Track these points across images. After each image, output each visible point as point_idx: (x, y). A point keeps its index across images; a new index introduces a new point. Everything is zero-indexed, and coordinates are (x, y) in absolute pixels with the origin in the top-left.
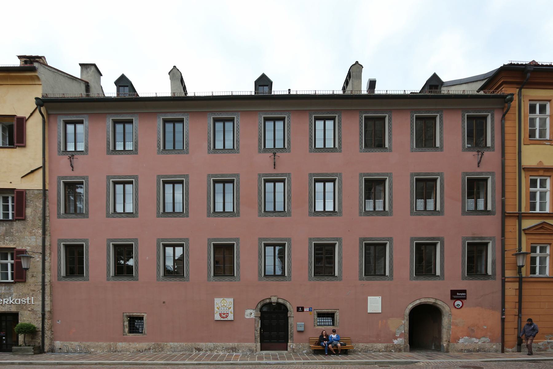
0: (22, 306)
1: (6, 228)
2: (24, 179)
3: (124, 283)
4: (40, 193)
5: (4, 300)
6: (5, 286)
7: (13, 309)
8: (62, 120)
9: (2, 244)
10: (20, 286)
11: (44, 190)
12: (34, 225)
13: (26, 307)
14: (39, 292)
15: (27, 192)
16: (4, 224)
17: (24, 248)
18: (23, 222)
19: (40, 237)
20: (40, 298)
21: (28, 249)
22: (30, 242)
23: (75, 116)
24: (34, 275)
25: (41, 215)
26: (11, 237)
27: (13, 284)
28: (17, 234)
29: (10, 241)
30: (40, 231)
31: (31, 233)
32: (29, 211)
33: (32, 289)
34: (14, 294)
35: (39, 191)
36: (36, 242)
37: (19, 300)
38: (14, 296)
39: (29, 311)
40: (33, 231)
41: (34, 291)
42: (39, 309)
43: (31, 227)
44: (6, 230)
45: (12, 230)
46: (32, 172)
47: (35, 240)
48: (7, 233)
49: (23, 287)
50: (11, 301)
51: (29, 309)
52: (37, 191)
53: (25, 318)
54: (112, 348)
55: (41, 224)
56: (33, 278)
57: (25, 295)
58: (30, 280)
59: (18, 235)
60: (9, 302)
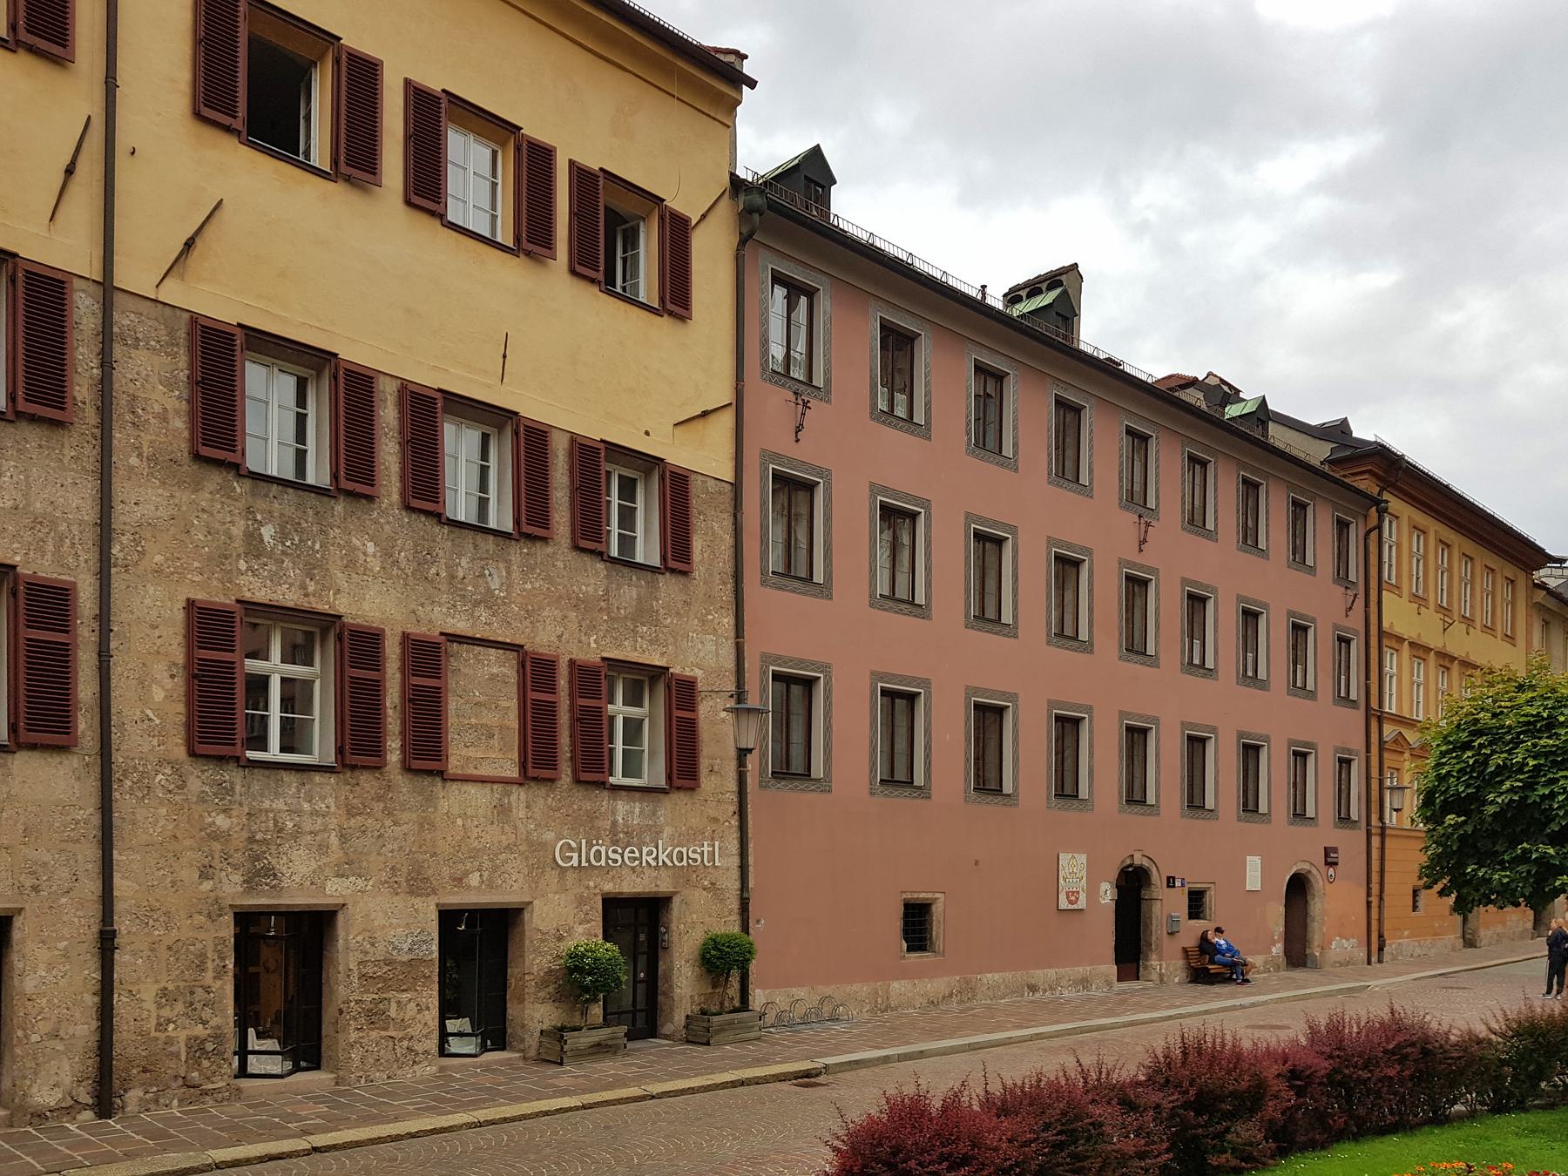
0: (687, 874)
1: (639, 595)
2: (679, 428)
3: (900, 802)
4: (720, 493)
5: (645, 850)
6: (641, 801)
7: (664, 887)
8: (770, 266)
9: (629, 649)
10: (679, 799)
11: (737, 486)
12: (709, 597)
13: (697, 876)
14: (727, 824)
15: (693, 477)
16: (634, 578)
17: (687, 673)
18: (682, 579)
19: (727, 639)
20: (733, 846)
21: (698, 673)
22: (701, 654)
23: (792, 265)
24: (716, 768)
25: (729, 568)
26: (653, 629)
27: (661, 796)
28: (669, 621)
29: (651, 642)
30: (728, 621)
31: (703, 622)
32: (698, 544)
33: (712, 813)
34: (668, 831)
35: (717, 482)
36: (718, 655)
37: (684, 850)
38: (665, 836)
39: (704, 889)
40: (710, 617)
41: (715, 820)
42: (732, 883)
43: (705, 602)
44: (639, 599)
45: (655, 603)
46: (705, 414)
47: (714, 648)
48: (643, 613)
49: (689, 805)
50: (662, 857)
51: (706, 883)
52: (713, 481)
53: (695, 916)
54: (879, 1001)
55: (727, 594)
56: (713, 778)
57: (693, 836)
58: (707, 783)
59: (672, 622)
60: (656, 858)
